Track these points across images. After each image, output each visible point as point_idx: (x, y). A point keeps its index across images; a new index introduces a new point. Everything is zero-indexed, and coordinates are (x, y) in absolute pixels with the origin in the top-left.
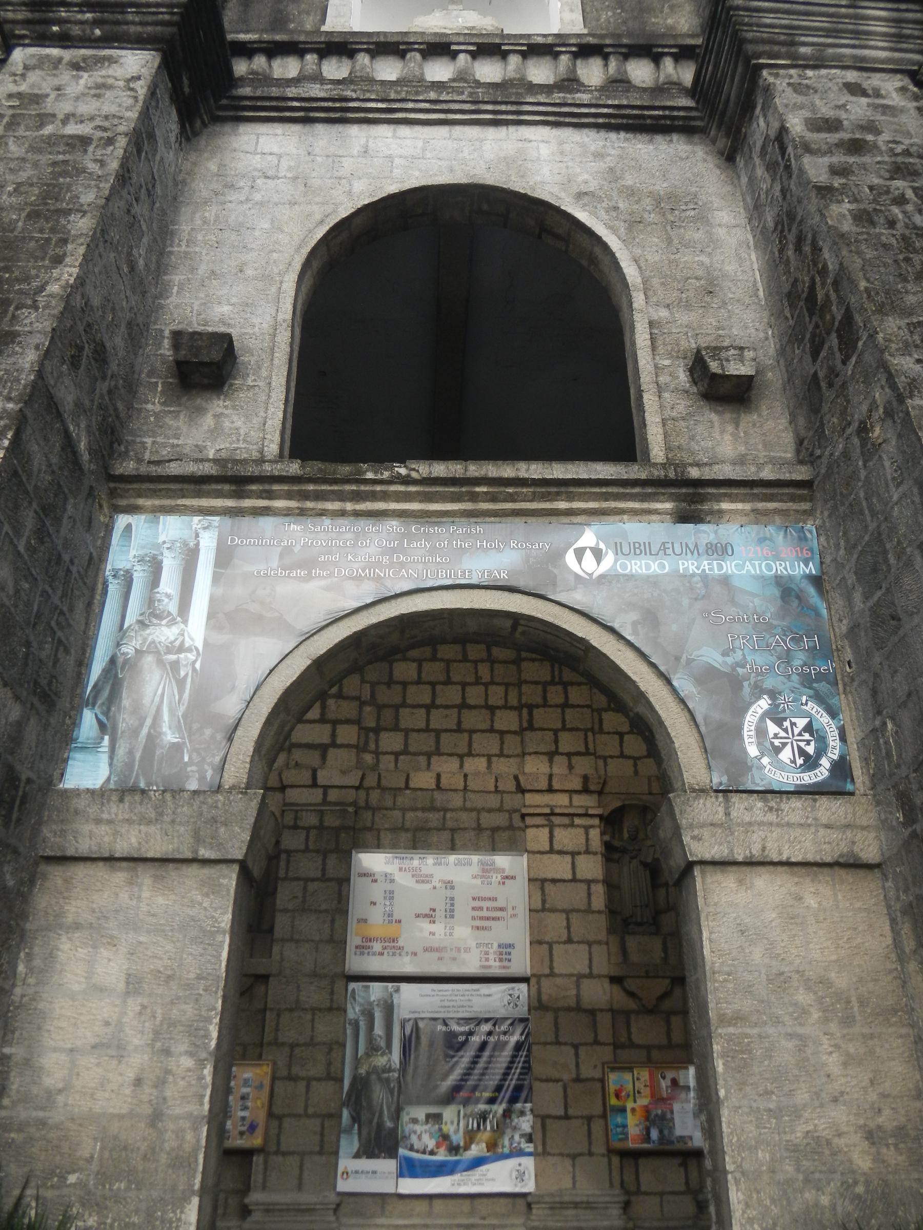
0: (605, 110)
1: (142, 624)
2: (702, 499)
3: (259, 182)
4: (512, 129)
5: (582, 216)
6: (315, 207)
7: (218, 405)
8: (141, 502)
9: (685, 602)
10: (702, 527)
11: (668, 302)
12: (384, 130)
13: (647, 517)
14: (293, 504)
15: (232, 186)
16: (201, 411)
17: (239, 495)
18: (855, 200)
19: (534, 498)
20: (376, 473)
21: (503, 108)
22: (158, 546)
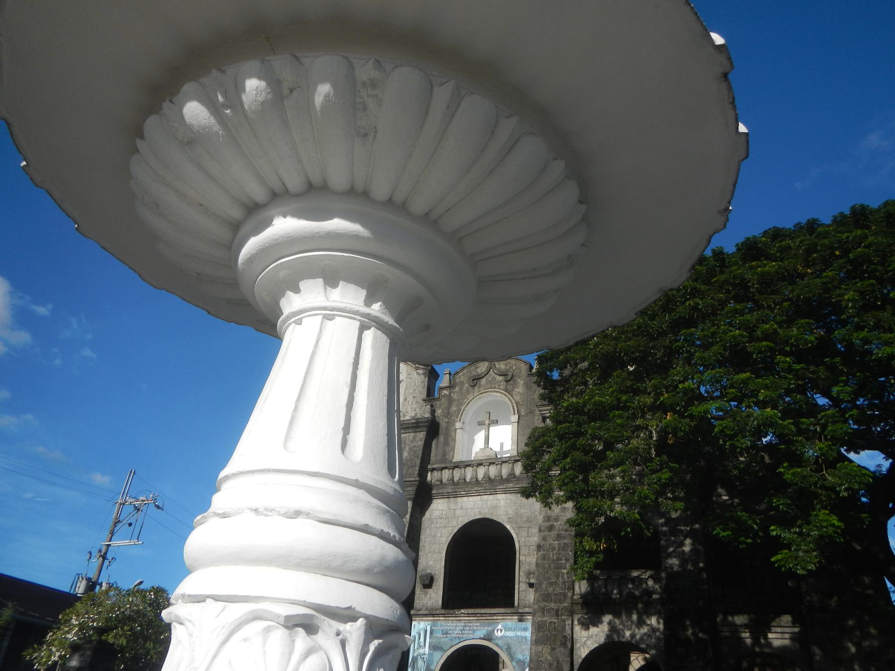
0: (517, 489)
1: (418, 649)
2: (523, 616)
3: (438, 520)
4: (495, 495)
5: (508, 527)
6: (450, 528)
7: (430, 590)
8: (416, 618)
9: (517, 643)
10: (523, 623)
11: (525, 554)
12: (465, 499)
13: (512, 620)
14: (444, 618)
15: (432, 522)
16: (426, 593)
17: (434, 617)
18: (544, 551)
19: (489, 616)
20: (458, 612)
21: (492, 491)
22: (420, 629)
